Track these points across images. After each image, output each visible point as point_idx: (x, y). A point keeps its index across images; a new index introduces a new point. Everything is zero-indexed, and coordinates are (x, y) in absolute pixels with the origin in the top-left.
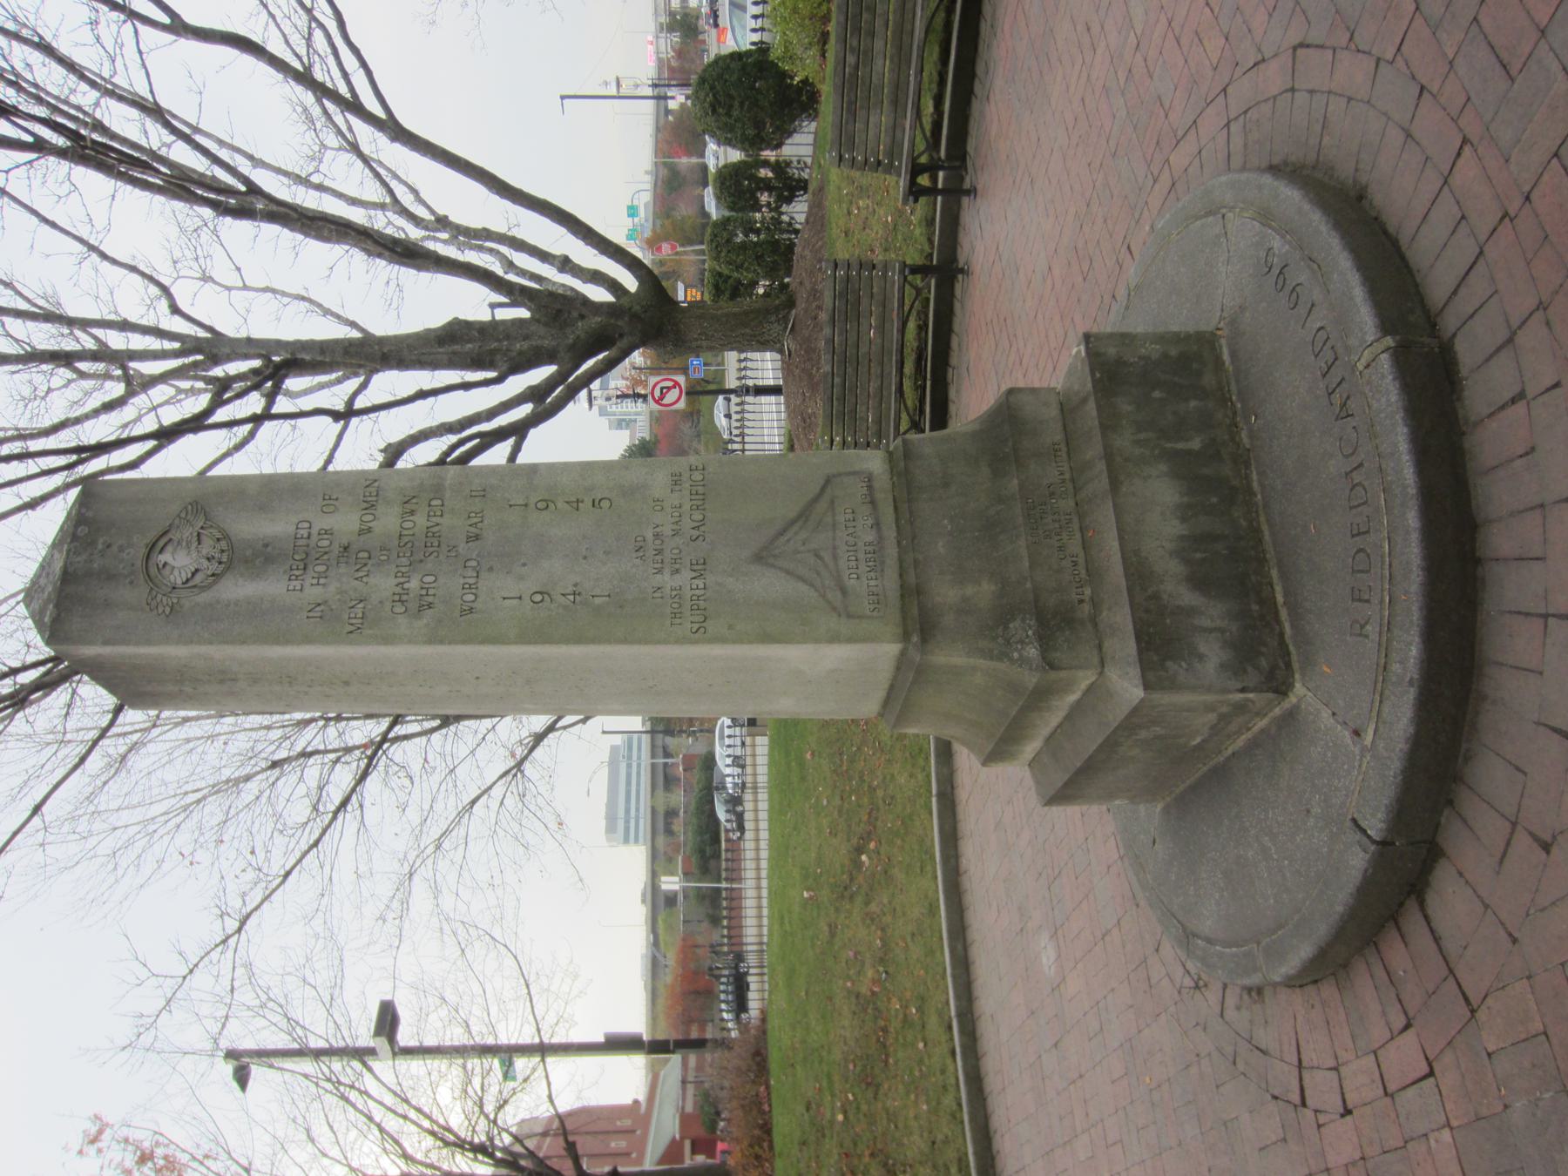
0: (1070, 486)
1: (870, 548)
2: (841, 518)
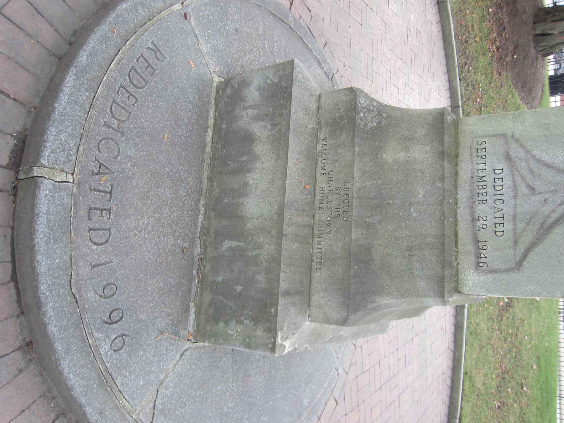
0: (316, 232)
1: (481, 197)
2: (508, 226)
